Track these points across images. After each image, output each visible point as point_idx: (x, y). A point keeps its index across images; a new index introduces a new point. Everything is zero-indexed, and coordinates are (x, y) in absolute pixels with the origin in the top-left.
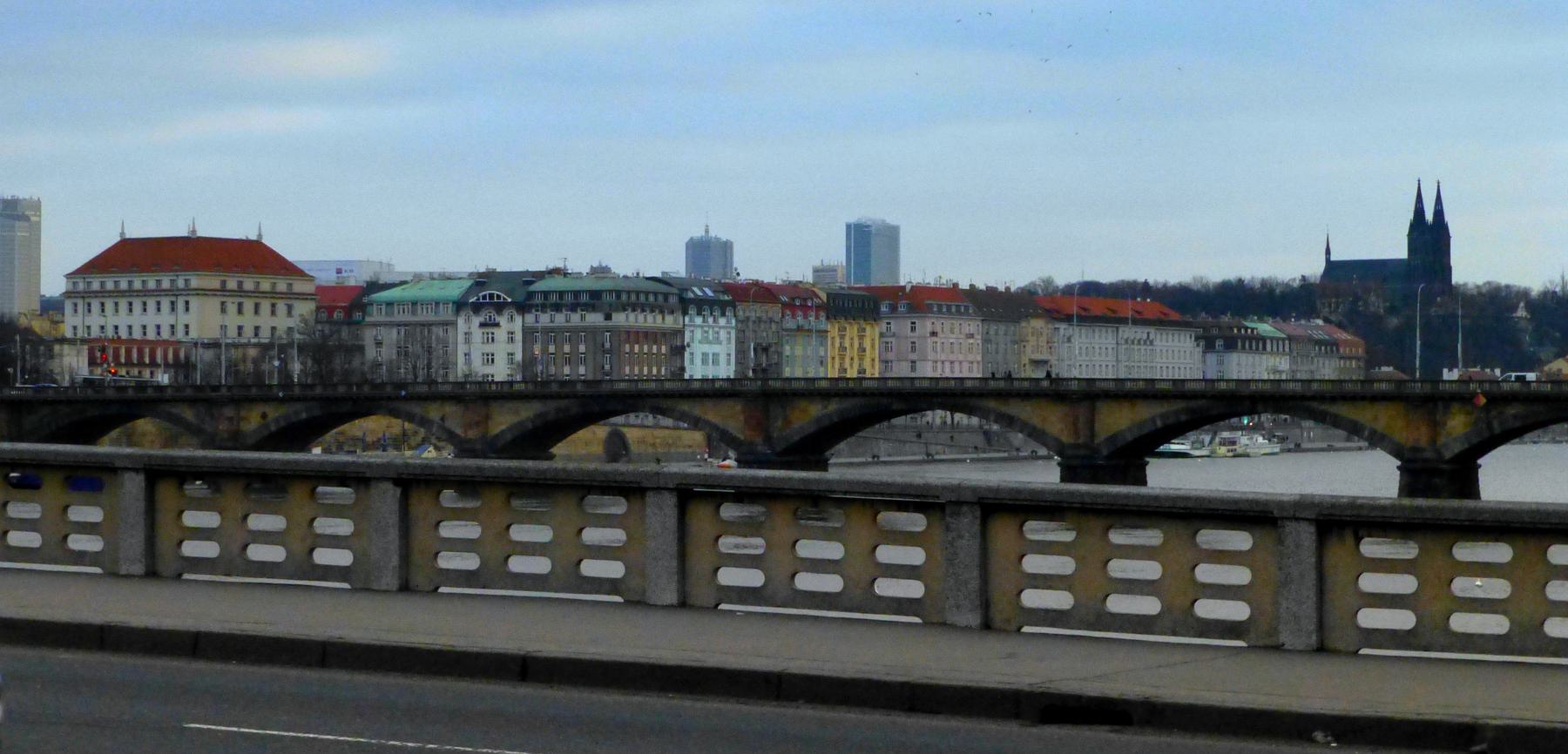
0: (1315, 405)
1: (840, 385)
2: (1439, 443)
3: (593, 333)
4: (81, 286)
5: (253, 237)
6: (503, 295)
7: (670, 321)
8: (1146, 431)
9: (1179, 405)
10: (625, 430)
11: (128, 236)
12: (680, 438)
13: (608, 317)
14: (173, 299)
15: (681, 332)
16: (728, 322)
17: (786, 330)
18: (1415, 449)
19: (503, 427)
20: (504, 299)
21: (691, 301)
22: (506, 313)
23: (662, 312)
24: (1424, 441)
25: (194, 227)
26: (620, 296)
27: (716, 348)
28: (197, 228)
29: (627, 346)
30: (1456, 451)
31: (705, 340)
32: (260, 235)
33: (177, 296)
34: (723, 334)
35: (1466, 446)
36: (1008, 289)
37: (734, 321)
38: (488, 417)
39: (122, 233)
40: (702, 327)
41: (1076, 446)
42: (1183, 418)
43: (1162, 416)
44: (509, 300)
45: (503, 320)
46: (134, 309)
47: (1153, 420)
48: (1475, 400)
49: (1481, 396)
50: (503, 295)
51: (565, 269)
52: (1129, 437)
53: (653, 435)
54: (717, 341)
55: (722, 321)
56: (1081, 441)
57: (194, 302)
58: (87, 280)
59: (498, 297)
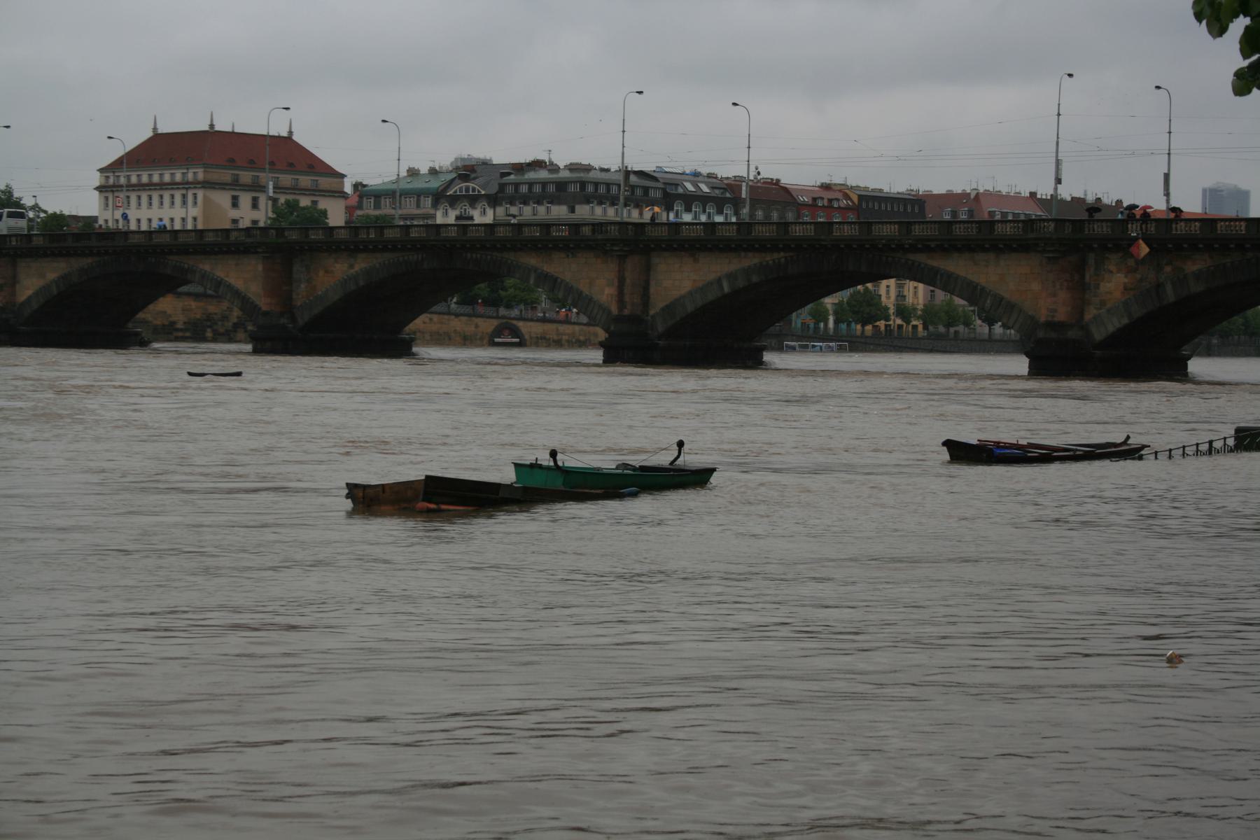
0: (921, 258)
2: (1088, 316)
4: (111, 181)
5: (285, 134)
6: (477, 187)
8: (712, 296)
9: (751, 260)
10: (520, 324)
11: (160, 131)
13: (572, 210)
14: (184, 192)
18: (1050, 325)
19: (30, 292)
20: (479, 191)
21: (679, 196)
22: (479, 206)
23: (637, 206)
24: (1062, 315)
30: (1111, 329)
32: (291, 132)
33: (187, 189)
35: (1125, 321)
36: (1119, 202)
38: (14, 281)
39: (155, 129)
42: (755, 279)
43: (731, 276)
44: (483, 193)
46: (164, 203)
47: (719, 281)
48: (1133, 250)
49: (1141, 241)
50: (477, 187)
51: (552, 163)
52: (690, 308)
53: (557, 330)
56: (626, 312)
57: (200, 194)
58: (116, 174)
59: (474, 190)
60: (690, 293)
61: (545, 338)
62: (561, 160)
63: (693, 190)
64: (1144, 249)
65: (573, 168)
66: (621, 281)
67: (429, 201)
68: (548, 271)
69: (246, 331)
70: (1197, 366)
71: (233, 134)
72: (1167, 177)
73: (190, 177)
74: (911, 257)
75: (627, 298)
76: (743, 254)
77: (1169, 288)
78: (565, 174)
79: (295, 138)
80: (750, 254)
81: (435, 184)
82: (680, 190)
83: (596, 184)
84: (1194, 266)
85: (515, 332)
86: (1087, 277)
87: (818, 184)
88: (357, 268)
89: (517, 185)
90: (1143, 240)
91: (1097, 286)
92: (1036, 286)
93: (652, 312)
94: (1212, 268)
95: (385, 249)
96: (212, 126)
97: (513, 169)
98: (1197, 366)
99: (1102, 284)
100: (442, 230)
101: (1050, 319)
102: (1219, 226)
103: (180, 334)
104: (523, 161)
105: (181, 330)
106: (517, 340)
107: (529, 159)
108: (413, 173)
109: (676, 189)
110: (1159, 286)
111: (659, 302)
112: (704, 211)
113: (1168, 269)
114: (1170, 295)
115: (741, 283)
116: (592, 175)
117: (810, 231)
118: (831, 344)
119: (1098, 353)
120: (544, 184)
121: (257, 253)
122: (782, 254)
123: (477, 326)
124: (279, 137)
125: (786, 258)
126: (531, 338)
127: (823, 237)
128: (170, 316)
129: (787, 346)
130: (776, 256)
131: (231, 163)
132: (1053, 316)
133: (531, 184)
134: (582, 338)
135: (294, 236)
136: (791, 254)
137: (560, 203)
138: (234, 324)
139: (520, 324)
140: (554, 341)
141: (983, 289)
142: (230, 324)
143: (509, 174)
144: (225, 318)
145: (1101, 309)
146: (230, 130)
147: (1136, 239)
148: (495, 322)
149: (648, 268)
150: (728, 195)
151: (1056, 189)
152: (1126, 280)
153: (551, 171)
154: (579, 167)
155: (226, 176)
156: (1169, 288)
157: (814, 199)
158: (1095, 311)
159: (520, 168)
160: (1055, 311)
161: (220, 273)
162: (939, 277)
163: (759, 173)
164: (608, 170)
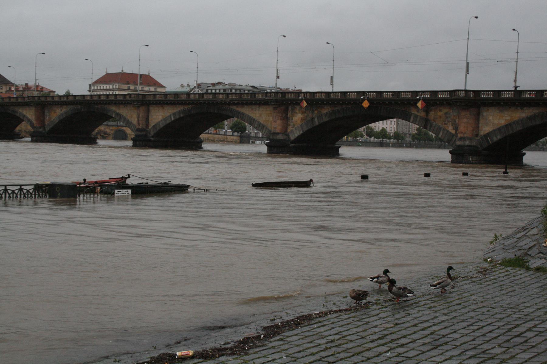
0: (234, 107)
1: (77, 99)
2: (289, 130)
5: (147, 74)
6: (200, 91)
8: (168, 122)
9: (180, 108)
12: (226, 138)
14: (112, 92)
18: (275, 134)
25: (123, 69)
28: (123, 70)
30: (296, 135)
32: (149, 73)
33: (113, 91)
35: (301, 132)
41: (138, 130)
42: (182, 115)
43: (174, 114)
44: (201, 92)
47: (171, 115)
48: (301, 104)
49: (304, 101)
51: (224, 83)
52: (161, 126)
53: (213, 137)
56: (140, 127)
60: (161, 120)
61: (208, 139)
64: (305, 104)
65: (230, 84)
66: (139, 115)
68: (119, 112)
70: (344, 151)
71: (132, 74)
72: (332, 78)
73: (114, 87)
74: (231, 107)
75: (140, 122)
76: (178, 106)
77: (316, 120)
78: (227, 87)
80: (180, 106)
81: (187, 89)
83: (236, 90)
84: (325, 110)
86: (289, 115)
88: (63, 111)
89: (211, 90)
90: (305, 100)
91: (292, 119)
92: (271, 119)
93: (150, 128)
94: (331, 112)
95: (73, 104)
96: (122, 71)
97: (212, 85)
98: (344, 151)
99: (294, 118)
100: (85, 97)
101: (274, 131)
102: (331, 95)
104: (215, 82)
108: (182, 86)
110: (313, 118)
111: (152, 124)
113: (316, 112)
114: (317, 122)
115: (177, 117)
117: (196, 97)
119: (292, 145)
120: (220, 90)
121: (31, 105)
122: (190, 106)
125: (191, 107)
126: (203, 139)
127: (200, 99)
130: (188, 106)
131: (128, 83)
132: (275, 130)
133: (216, 90)
134: (222, 139)
135: (43, 99)
136: (193, 106)
138: (97, 133)
140: (212, 140)
141: (254, 120)
142: (95, 133)
143: (210, 86)
145: (293, 127)
147: (302, 100)
149: (148, 112)
151: (277, 80)
152: (302, 116)
153: (223, 85)
154: (231, 84)
155: (126, 87)
156: (316, 120)
158: (291, 129)
159: (213, 85)
160: (275, 128)
161: (24, 113)
162: (240, 115)
164: (241, 85)
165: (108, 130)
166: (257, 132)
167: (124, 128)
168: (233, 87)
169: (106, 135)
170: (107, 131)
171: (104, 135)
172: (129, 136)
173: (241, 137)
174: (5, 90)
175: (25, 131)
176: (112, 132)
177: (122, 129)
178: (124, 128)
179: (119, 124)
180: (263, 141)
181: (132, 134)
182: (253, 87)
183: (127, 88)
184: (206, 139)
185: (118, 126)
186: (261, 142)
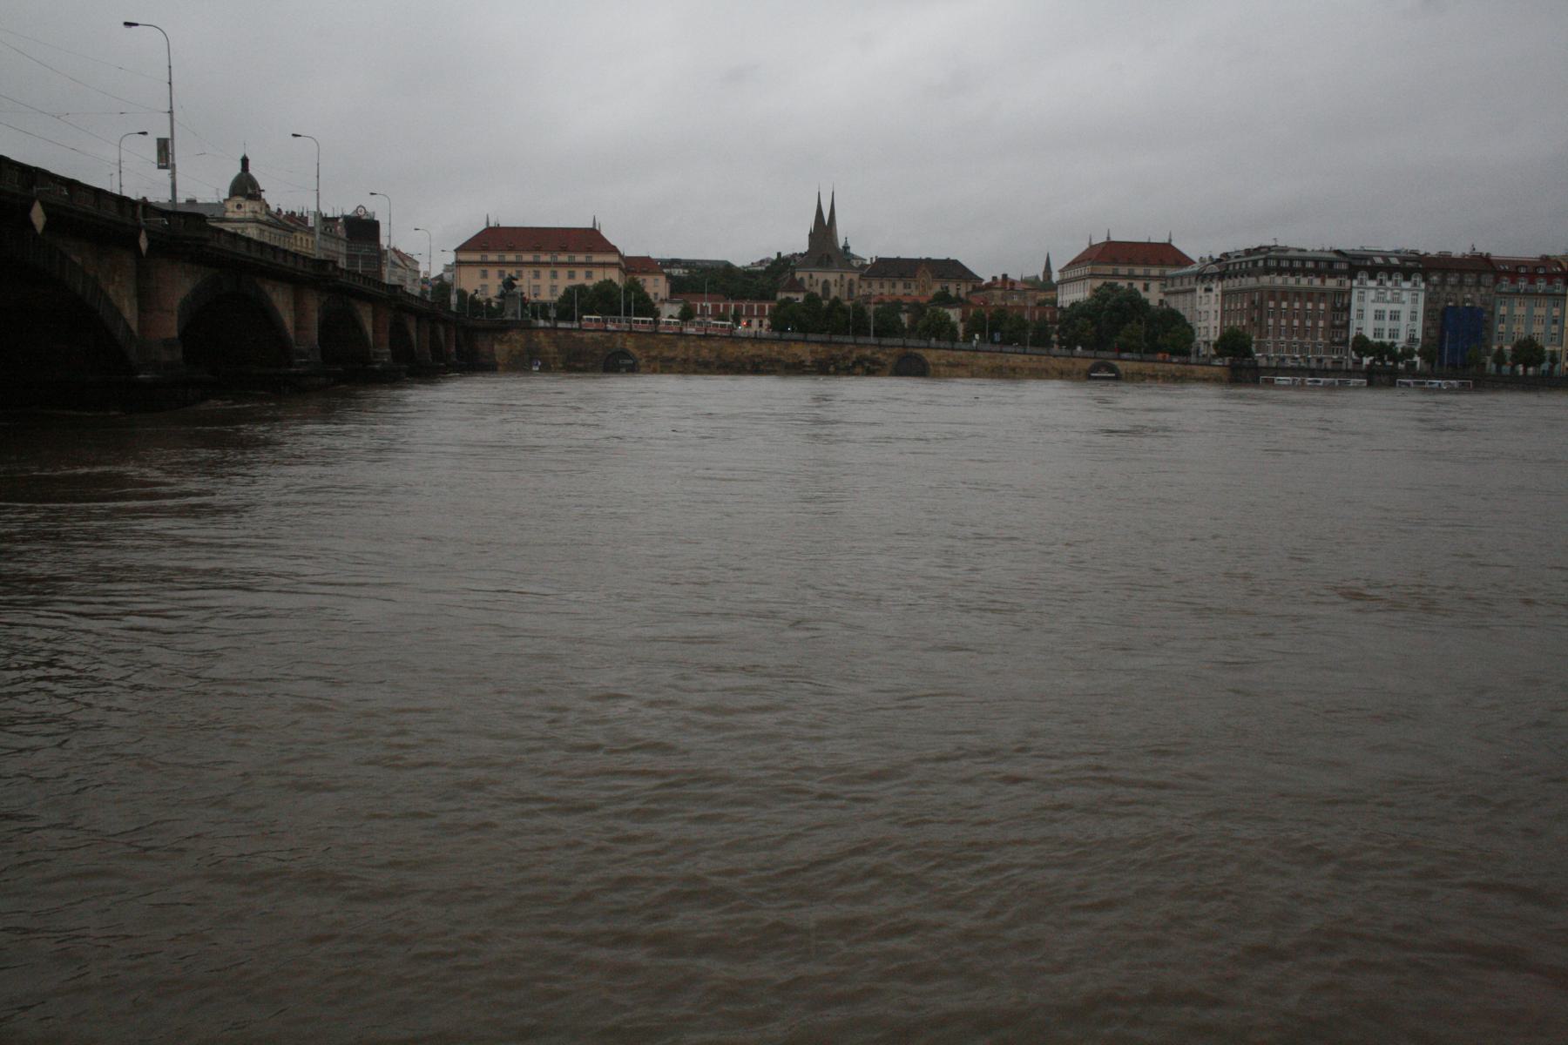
3: (1251, 291)
5: (1166, 241)
7: (1331, 283)
10: (1116, 363)
12: (1192, 372)
13: (1258, 281)
15: (1349, 292)
16: (1415, 285)
17: (1500, 293)
21: (1366, 268)
22: (1215, 281)
23: (1318, 276)
26: (1332, 266)
27: (1395, 307)
29: (1272, 304)
31: (1377, 300)
32: (1170, 240)
34: (1406, 296)
37: (1423, 285)
40: (1392, 290)
45: (1213, 286)
54: (1397, 300)
55: (1407, 285)
61: (1140, 374)
62: (1309, 249)
63: (1382, 262)
67: (1193, 279)
69: (863, 367)
71: (1149, 245)
79: (1173, 243)
82: (1369, 263)
85: (1111, 369)
87: (1538, 256)
96: (1108, 238)
103: (808, 369)
105: (809, 366)
106: (1113, 375)
107: (1256, 246)
109: (1366, 262)
112: (1390, 279)
116: (1290, 254)
118: (1452, 382)
123: (1074, 364)
124: (1164, 244)
126: (1126, 373)
128: (800, 356)
129: (1400, 382)
131: (1115, 261)
134: (1177, 374)
137: (1252, 276)
139: (1116, 363)
144: (845, 358)
146: (1146, 240)
148: (1092, 362)
150: (1420, 266)
157: (1517, 267)
163: (1474, 249)
164: (1305, 251)
165: (879, 355)
166: (1339, 358)
167: (921, 352)
168: (1282, 254)
169: (876, 367)
170: (878, 358)
171: (872, 367)
172: (931, 367)
173: (1233, 368)
174: (965, 291)
175: (696, 362)
176: (890, 360)
177: (916, 354)
178: (921, 352)
179: (947, 346)
180: (1299, 379)
181: (938, 365)
182: (1338, 252)
183: (1111, 273)
184: (1133, 373)
185: (904, 346)
186: (1294, 380)
